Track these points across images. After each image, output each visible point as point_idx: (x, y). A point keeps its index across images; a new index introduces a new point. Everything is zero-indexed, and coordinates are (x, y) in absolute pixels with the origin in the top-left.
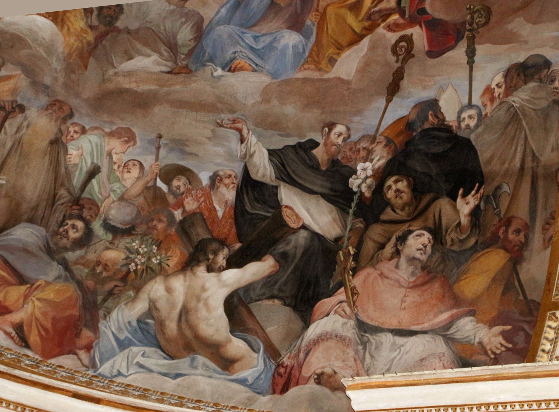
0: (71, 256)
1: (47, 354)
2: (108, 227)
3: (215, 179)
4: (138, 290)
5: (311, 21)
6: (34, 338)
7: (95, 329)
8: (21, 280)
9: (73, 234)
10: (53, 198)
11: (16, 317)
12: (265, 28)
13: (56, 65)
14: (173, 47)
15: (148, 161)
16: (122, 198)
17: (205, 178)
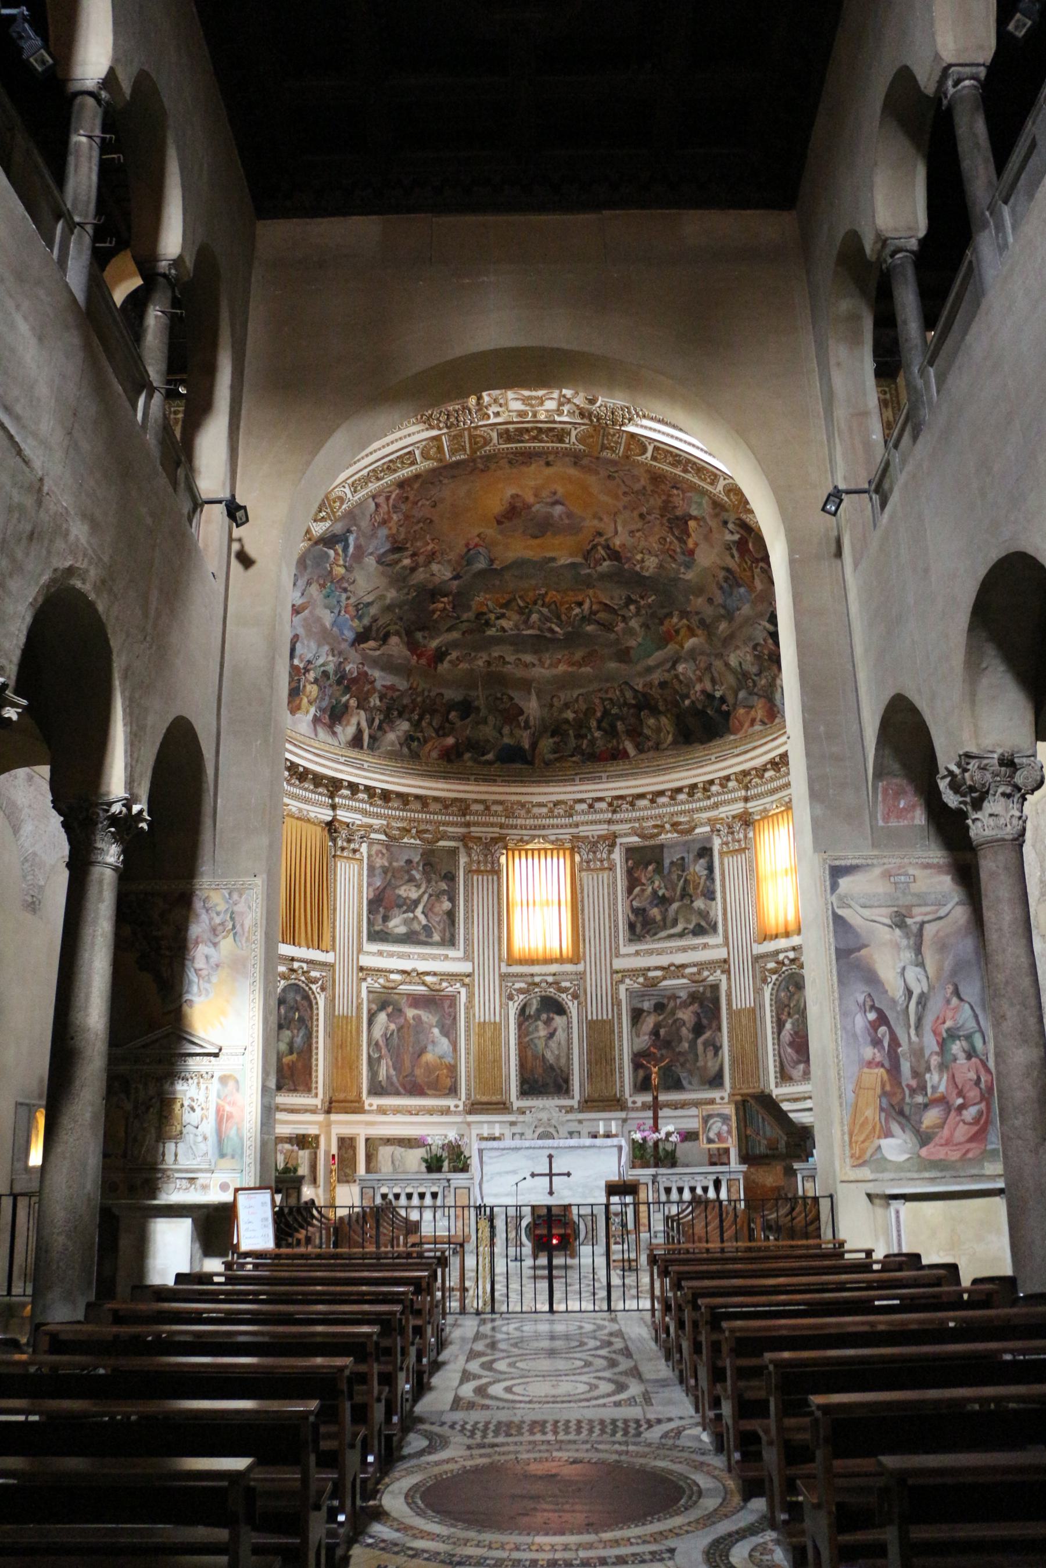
0: (756, 690)
1: (772, 722)
2: (756, 675)
3: (765, 640)
4: (775, 686)
5: (740, 582)
6: (766, 721)
7: (775, 705)
8: (752, 707)
9: (751, 684)
10: (738, 679)
11: (758, 719)
12: (735, 593)
13: (707, 646)
14: (723, 616)
15: (748, 649)
16: (753, 664)
17: (762, 642)
